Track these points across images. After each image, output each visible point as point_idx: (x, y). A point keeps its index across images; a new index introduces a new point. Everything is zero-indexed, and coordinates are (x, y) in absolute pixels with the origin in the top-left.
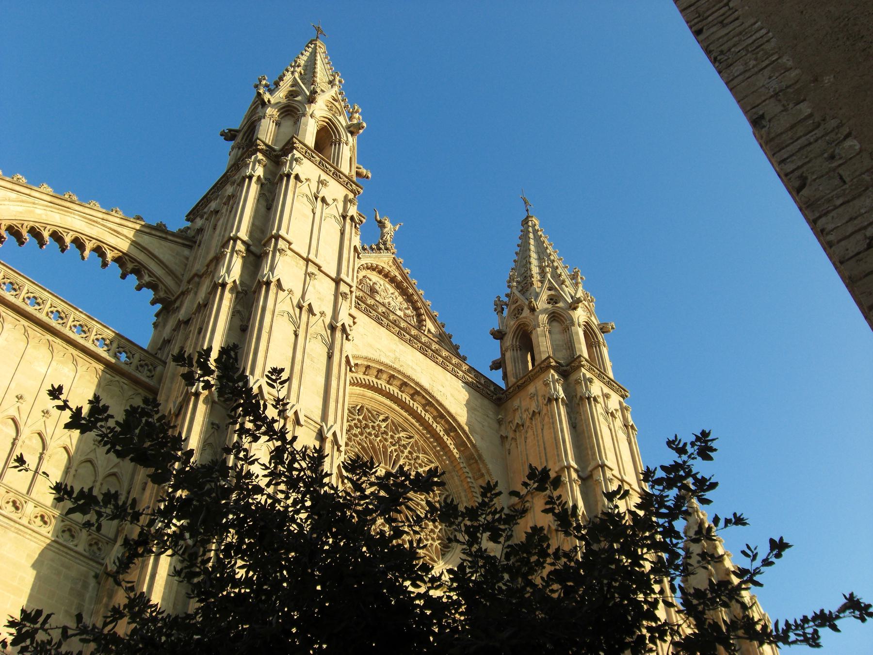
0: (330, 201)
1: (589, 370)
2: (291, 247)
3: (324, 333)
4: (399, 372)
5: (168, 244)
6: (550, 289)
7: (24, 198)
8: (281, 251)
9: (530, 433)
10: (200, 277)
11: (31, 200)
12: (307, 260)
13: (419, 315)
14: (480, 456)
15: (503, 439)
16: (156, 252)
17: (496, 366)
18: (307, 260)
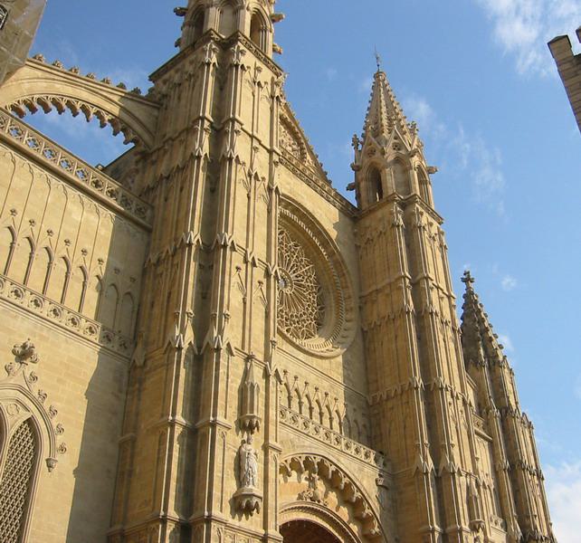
0: (263, 84)
1: (421, 205)
2: (243, 127)
3: (264, 194)
4: (293, 200)
5: (145, 107)
6: (395, 138)
7: (48, 75)
8: (237, 132)
9: (377, 246)
10: (173, 140)
11: (52, 76)
12: (252, 137)
13: (302, 149)
14: (343, 261)
15: (357, 247)
16: (137, 114)
17: (350, 188)
18: (252, 137)
